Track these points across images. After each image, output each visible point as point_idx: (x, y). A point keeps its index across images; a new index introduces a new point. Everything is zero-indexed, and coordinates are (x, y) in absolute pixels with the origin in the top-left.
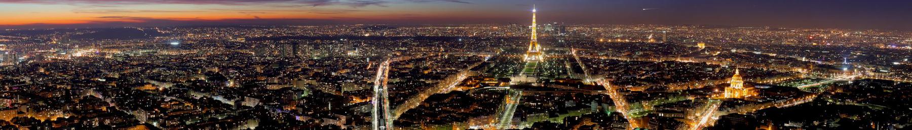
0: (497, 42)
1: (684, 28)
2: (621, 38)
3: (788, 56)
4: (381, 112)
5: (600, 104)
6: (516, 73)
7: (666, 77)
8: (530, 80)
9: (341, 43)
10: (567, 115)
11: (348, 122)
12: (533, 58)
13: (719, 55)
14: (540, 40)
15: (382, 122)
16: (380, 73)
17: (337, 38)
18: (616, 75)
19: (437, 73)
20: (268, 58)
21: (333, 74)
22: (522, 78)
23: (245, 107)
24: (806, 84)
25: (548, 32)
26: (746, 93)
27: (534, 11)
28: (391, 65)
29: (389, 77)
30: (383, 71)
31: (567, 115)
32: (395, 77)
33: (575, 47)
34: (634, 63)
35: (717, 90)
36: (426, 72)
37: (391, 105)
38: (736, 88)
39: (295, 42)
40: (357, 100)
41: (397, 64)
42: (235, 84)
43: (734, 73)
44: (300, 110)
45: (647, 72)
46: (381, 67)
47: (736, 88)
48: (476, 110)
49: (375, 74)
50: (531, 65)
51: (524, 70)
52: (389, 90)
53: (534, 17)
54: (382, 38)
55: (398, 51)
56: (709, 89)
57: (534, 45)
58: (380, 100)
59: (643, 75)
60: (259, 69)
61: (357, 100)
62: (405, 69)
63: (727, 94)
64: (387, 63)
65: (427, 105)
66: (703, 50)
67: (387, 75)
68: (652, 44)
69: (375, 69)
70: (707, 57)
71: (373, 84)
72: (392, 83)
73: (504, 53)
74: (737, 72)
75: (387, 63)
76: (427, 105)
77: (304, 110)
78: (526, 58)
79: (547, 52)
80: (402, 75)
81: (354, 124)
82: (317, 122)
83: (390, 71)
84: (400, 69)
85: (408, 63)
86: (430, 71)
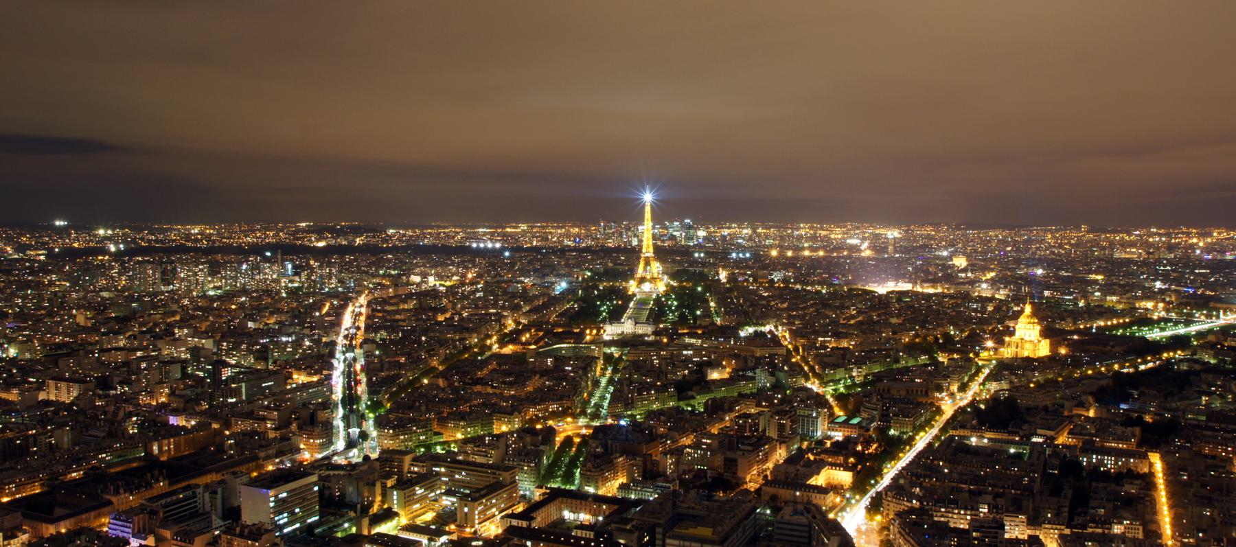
0: (579, 256)
1: (929, 230)
2: (811, 249)
3: (1124, 278)
4: (350, 399)
5: (772, 374)
6: (615, 316)
7: (894, 320)
8: (640, 330)
9: (267, 260)
10: (712, 396)
11: (282, 425)
12: (647, 287)
13: (992, 279)
15: (353, 418)
16: (347, 320)
17: (256, 250)
18: (802, 318)
19: (462, 319)
20: (105, 294)
21: (250, 324)
22: (627, 327)
23: (47, 403)
24: (1162, 329)
25: (673, 238)
26: (1044, 349)
27: (648, 197)
28: (369, 304)
30: (354, 316)
31: (712, 396)
32: (376, 330)
33: (724, 267)
34: (834, 295)
35: (990, 344)
36: (441, 318)
37: (370, 383)
38: (1028, 338)
40: (300, 378)
41: (385, 301)
42: (21, 352)
43: (1022, 312)
45: (859, 312)
46: (350, 308)
47: (1028, 338)
48: (539, 390)
49: (337, 324)
50: (642, 303)
51: (629, 312)
52: (368, 355)
53: (648, 209)
54: (350, 249)
55: (384, 276)
56: (974, 341)
57: (647, 263)
58: (349, 375)
59: (853, 317)
60: (81, 319)
61: (300, 378)
62: (398, 312)
63: (1007, 353)
64: (363, 300)
65: (441, 382)
66: (965, 270)
67: (362, 325)
68: (869, 258)
69: (338, 312)
70: (972, 282)
71: (334, 344)
72: (373, 341)
73: (591, 278)
74: (1028, 309)
75: (363, 300)
76: (441, 382)
78: (632, 287)
79: (673, 276)
80: (393, 327)
81: (294, 427)
83: (368, 317)
84: (388, 312)
85: (404, 301)
86: (448, 315)
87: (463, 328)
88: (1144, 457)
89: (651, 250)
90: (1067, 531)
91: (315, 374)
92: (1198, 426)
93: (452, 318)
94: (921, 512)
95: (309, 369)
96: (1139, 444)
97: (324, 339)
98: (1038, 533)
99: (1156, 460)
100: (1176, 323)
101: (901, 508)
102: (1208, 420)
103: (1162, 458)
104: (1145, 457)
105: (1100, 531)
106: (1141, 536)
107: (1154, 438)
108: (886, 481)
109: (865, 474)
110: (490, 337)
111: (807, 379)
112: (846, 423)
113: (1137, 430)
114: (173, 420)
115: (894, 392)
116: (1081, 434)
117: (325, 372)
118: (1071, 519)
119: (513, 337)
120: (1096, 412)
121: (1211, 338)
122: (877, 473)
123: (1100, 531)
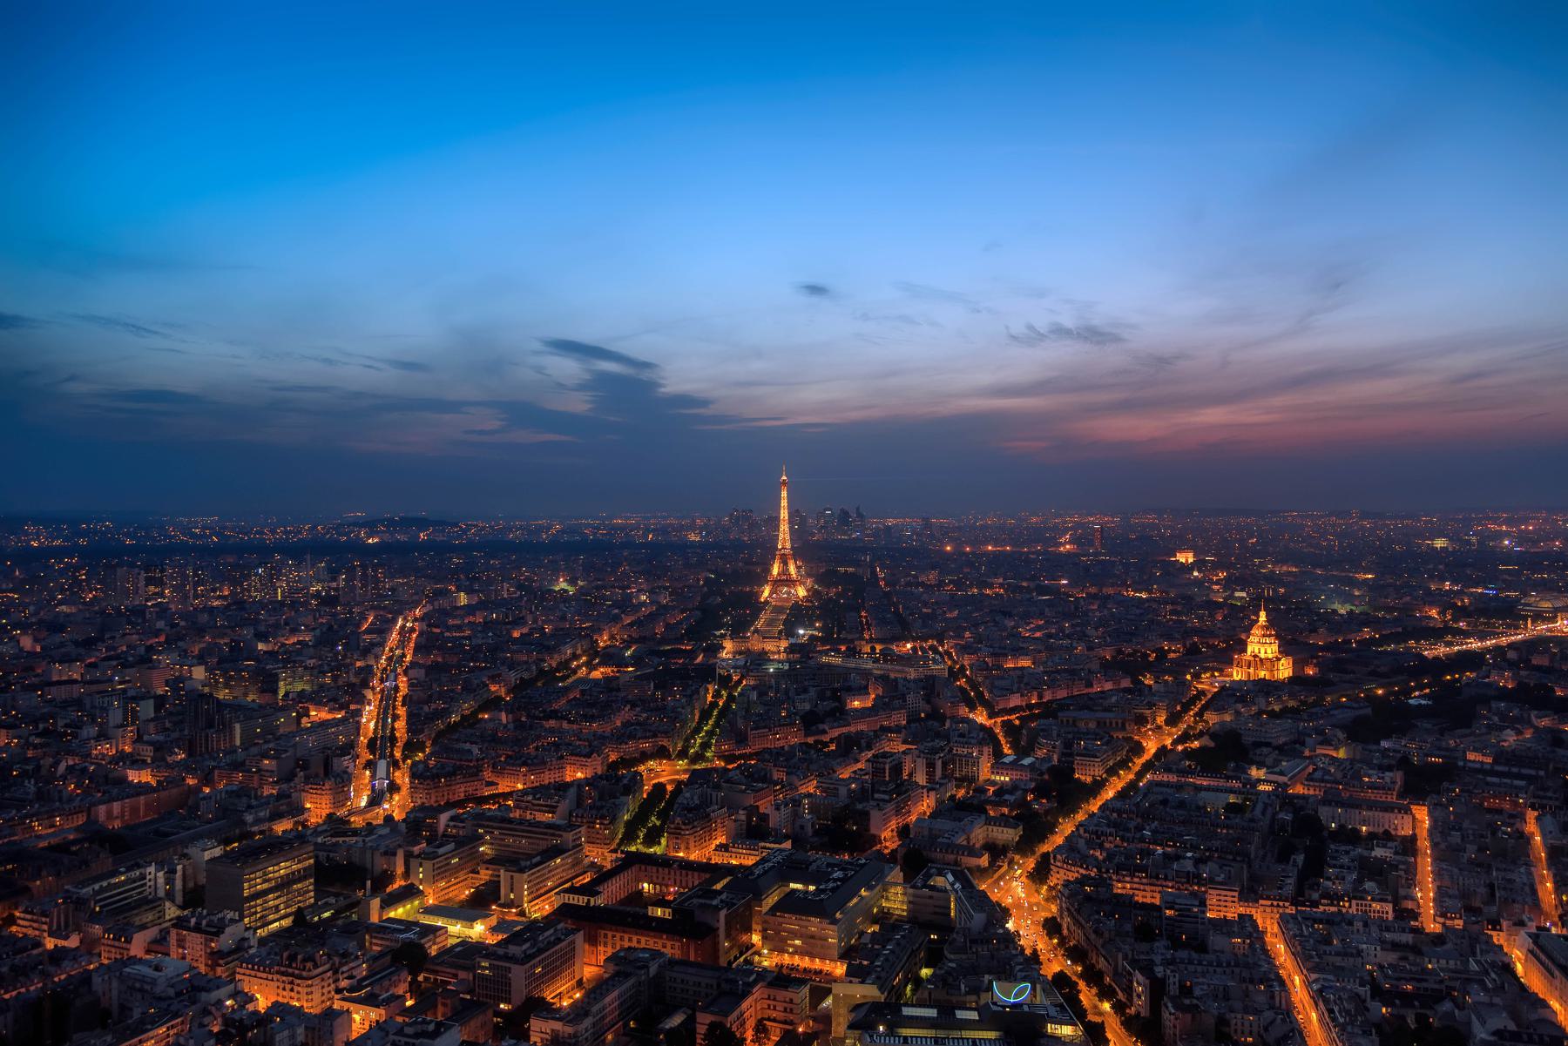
14: (799, 552)
29: (417, 649)
39: (155, 558)
44: (148, 753)
62: (459, 628)
71: (368, 670)
77: (159, 748)
82: (191, 782)
86: (525, 630)
87: (545, 646)
88: (1407, 810)
89: (788, 545)
90: (1291, 910)
91: (340, 709)
92: (1482, 770)
93: (530, 634)
94: (1099, 882)
95: (335, 702)
96: (1401, 796)
97: (358, 664)
98: (1253, 911)
99: (1422, 814)
100: (1466, 634)
101: (1072, 876)
102: (1495, 761)
103: (1430, 814)
104: (1407, 811)
105: (1333, 909)
106: (1390, 917)
107: (1421, 784)
108: (1059, 840)
109: (1035, 829)
110: (575, 657)
111: (972, 708)
112: (1014, 765)
113: (1398, 776)
114: (134, 776)
115: (1082, 725)
116: (1322, 781)
117: (352, 707)
118: (1300, 890)
119: (609, 657)
120: (1347, 752)
121: (1511, 655)
122: (1050, 829)
123: (1333, 909)
